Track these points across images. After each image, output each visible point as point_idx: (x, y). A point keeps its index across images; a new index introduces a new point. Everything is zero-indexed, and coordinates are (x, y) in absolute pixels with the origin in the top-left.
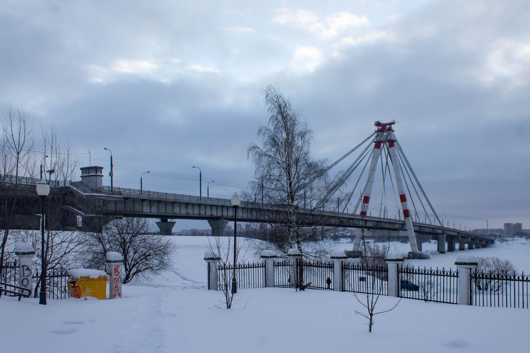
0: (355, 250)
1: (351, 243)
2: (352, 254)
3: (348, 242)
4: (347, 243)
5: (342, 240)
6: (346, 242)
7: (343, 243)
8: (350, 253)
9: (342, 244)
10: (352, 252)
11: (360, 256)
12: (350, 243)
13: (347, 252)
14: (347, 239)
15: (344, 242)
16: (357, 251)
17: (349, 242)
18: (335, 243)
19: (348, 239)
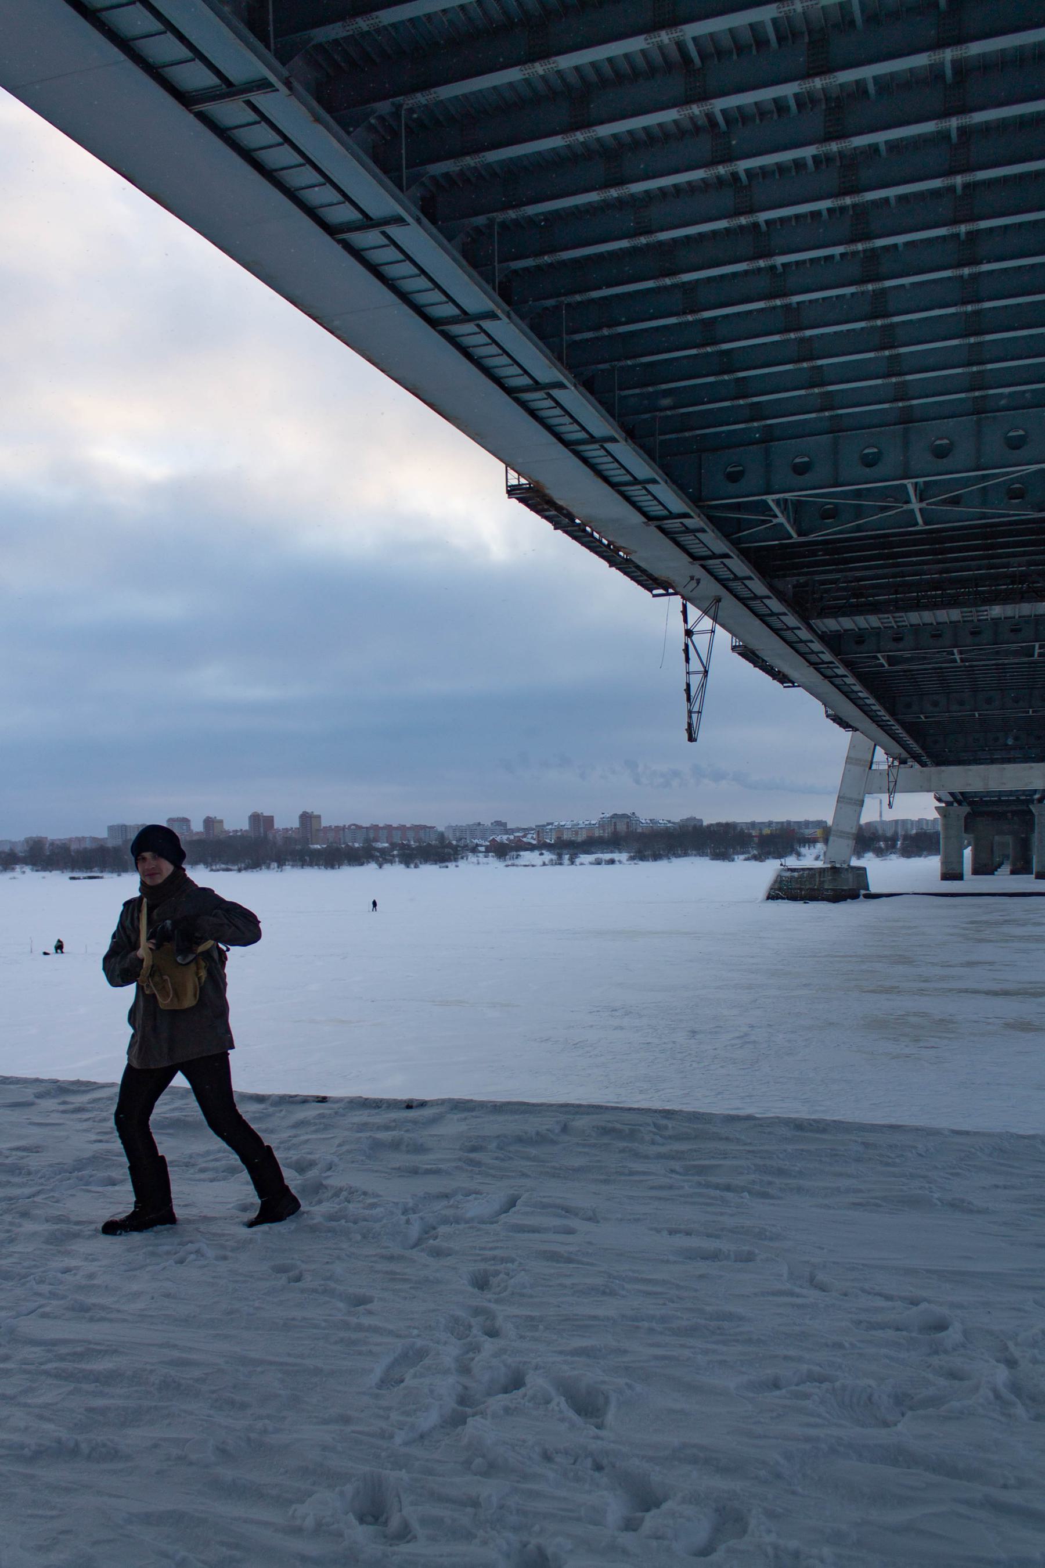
0: (838, 866)
1: (556, 864)
2: (822, 883)
3: (547, 863)
4: (544, 864)
5: (527, 856)
6: (541, 863)
7: (533, 866)
8: (812, 876)
9: (530, 868)
10: (822, 871)
11: (863, 892)
12: (552, 865)
13: (796, 874)
14: (542, 854)
15: (532, 863)
16: (845, 866)
17: (552, 863)
18: (507, 866)
19: (544, 852)
